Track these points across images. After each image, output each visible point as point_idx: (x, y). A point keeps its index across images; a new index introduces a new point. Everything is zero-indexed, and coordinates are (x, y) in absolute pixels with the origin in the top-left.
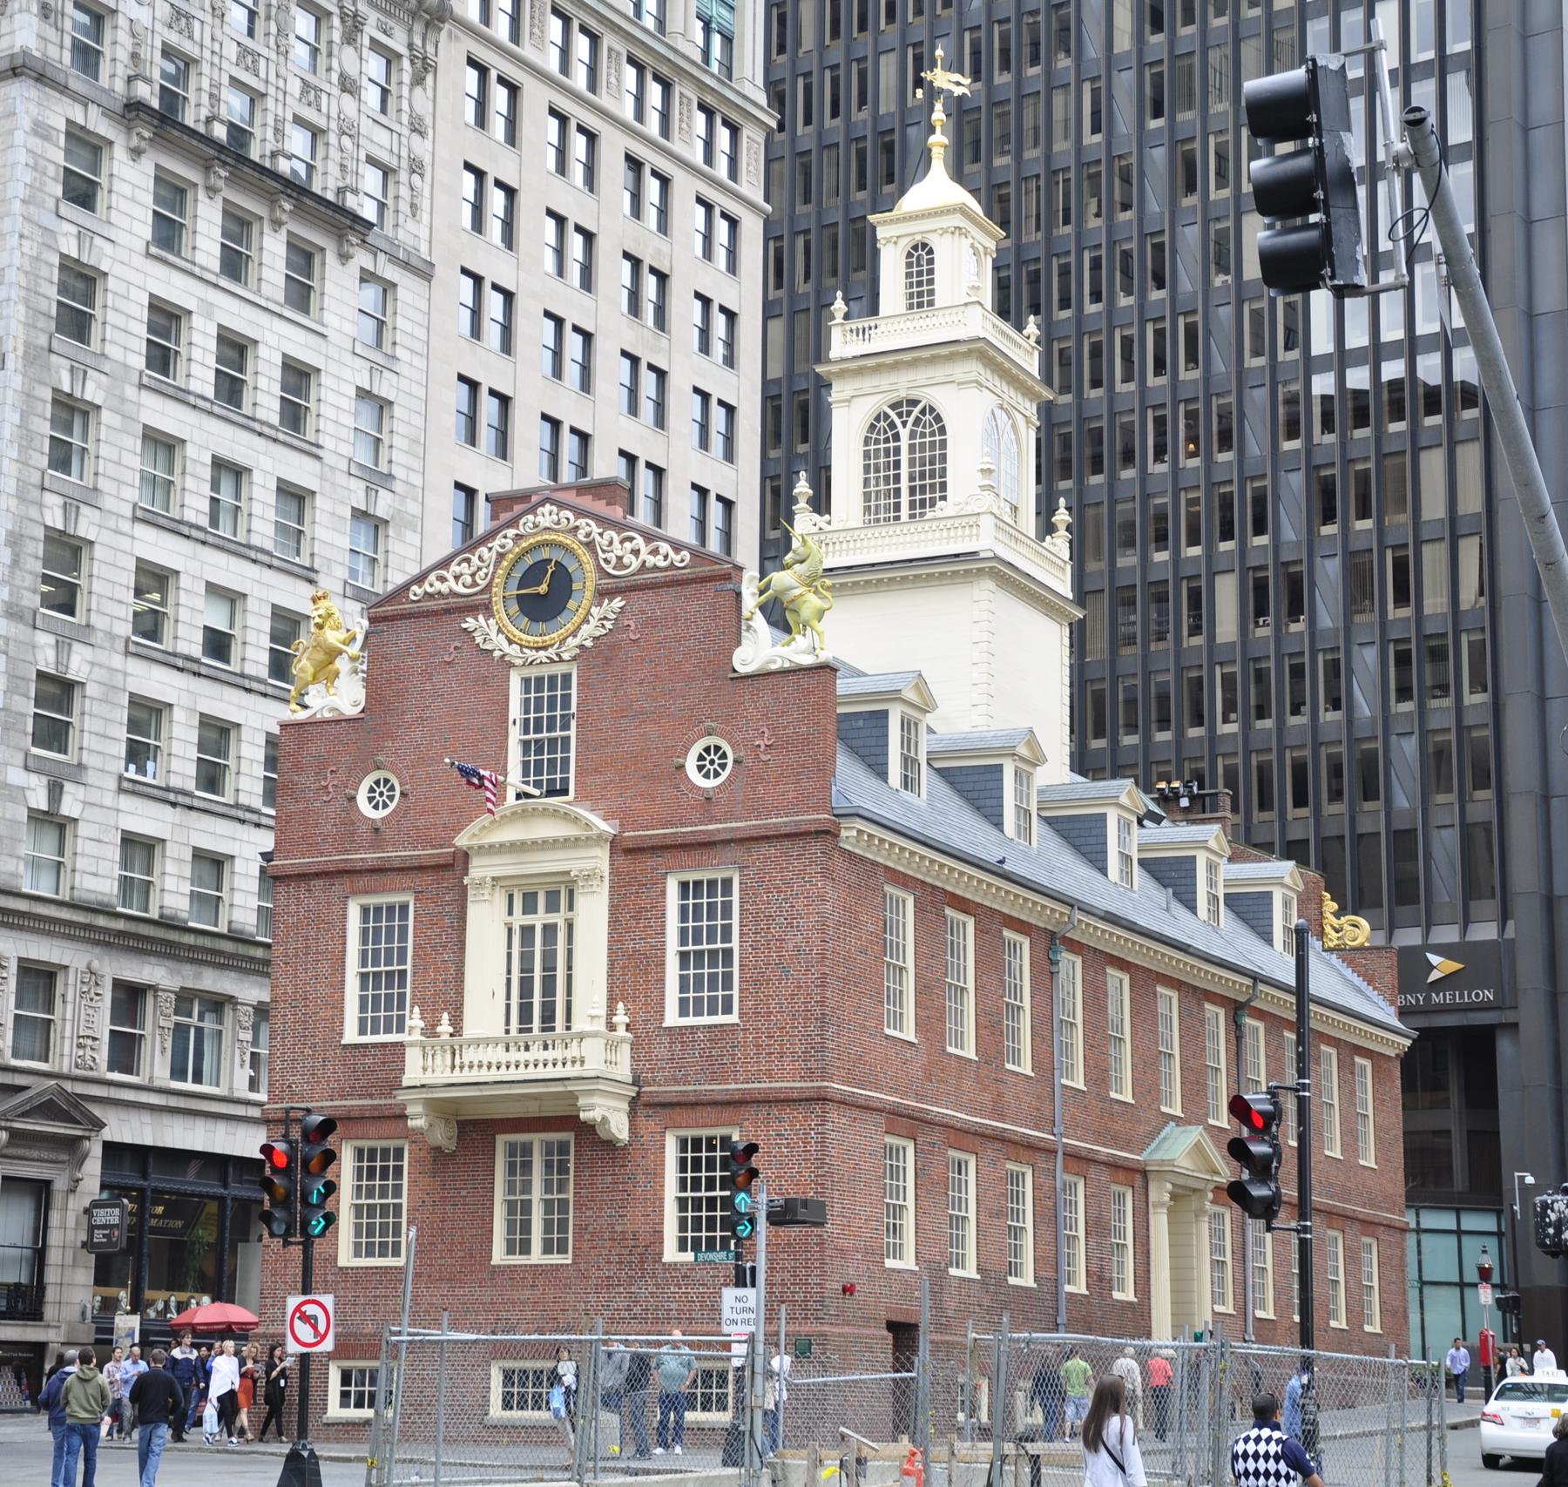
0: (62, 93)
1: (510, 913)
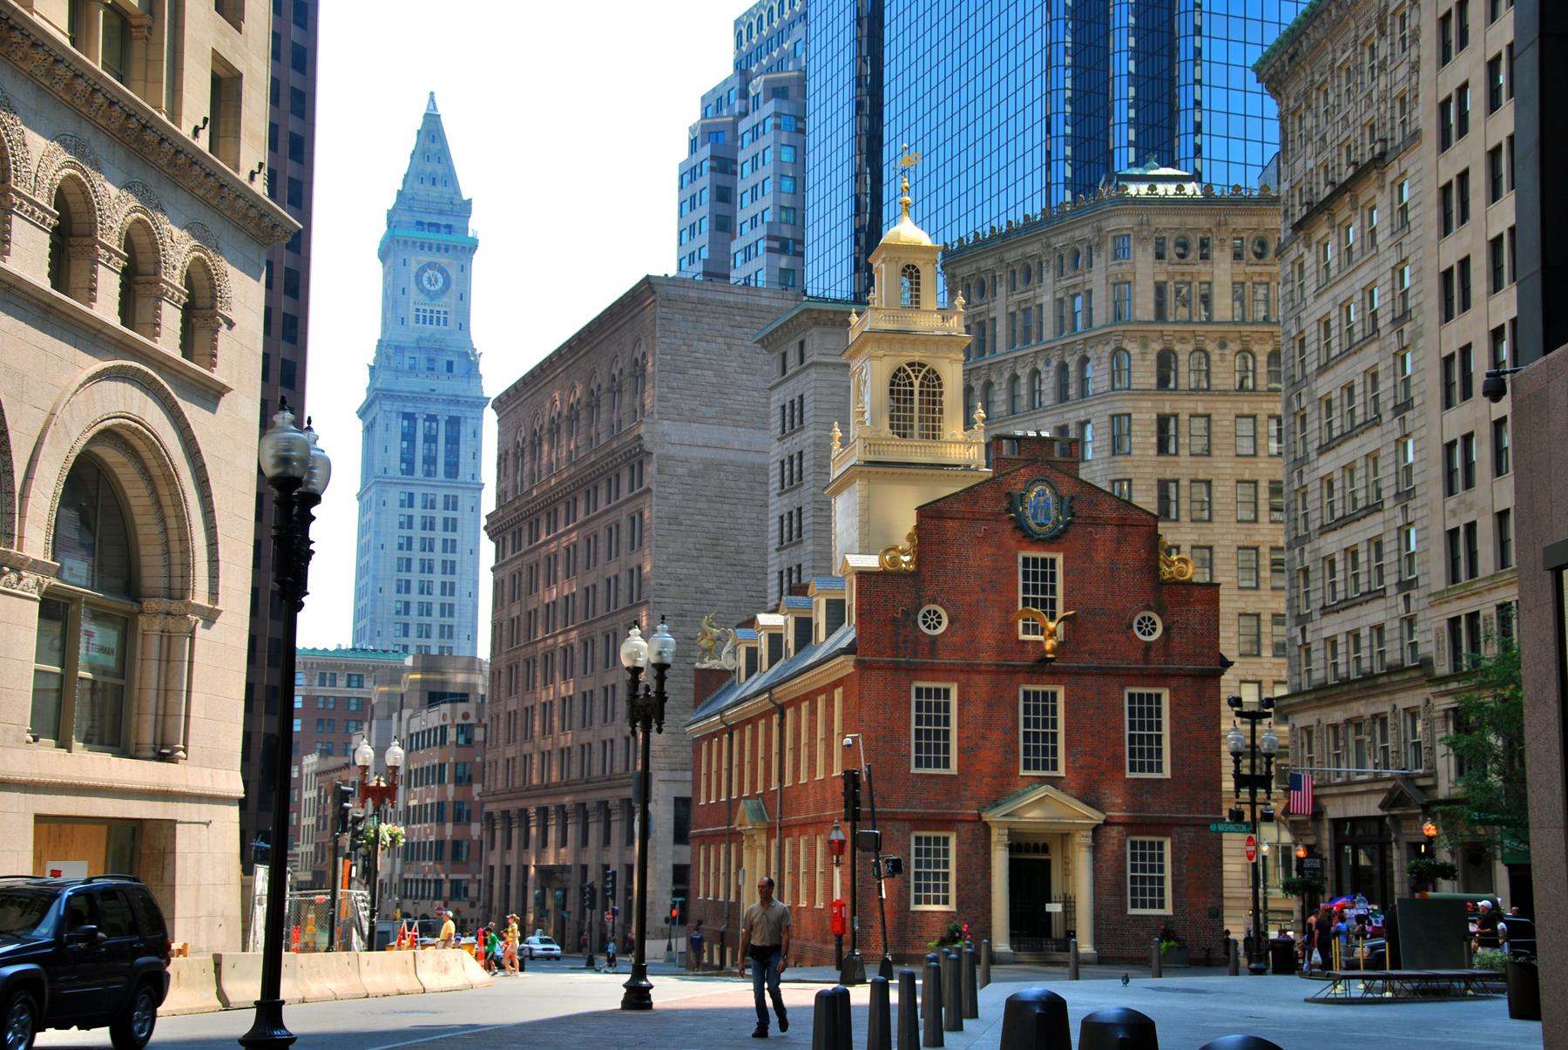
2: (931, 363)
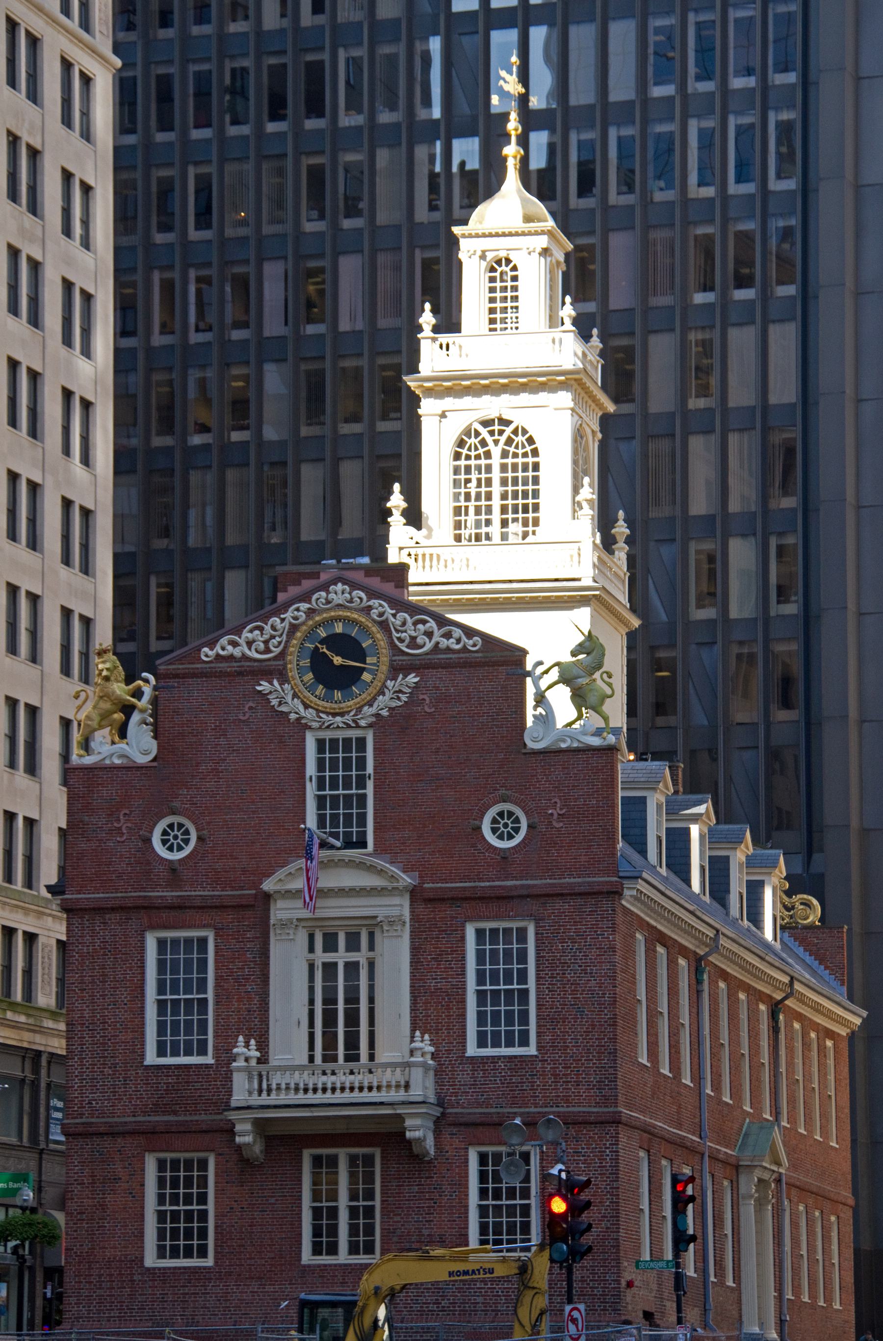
1: (311, 949)
2: (519, 419)
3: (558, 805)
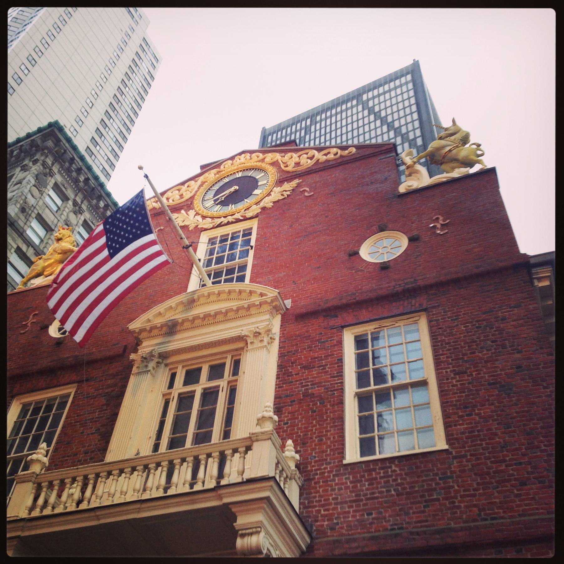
0: (19, 236)
1: (171, 385)
3: (441, 218)
